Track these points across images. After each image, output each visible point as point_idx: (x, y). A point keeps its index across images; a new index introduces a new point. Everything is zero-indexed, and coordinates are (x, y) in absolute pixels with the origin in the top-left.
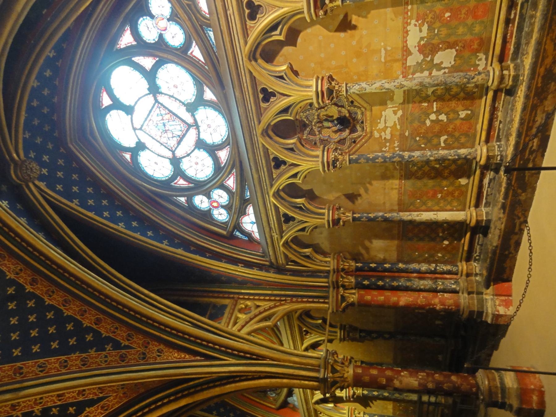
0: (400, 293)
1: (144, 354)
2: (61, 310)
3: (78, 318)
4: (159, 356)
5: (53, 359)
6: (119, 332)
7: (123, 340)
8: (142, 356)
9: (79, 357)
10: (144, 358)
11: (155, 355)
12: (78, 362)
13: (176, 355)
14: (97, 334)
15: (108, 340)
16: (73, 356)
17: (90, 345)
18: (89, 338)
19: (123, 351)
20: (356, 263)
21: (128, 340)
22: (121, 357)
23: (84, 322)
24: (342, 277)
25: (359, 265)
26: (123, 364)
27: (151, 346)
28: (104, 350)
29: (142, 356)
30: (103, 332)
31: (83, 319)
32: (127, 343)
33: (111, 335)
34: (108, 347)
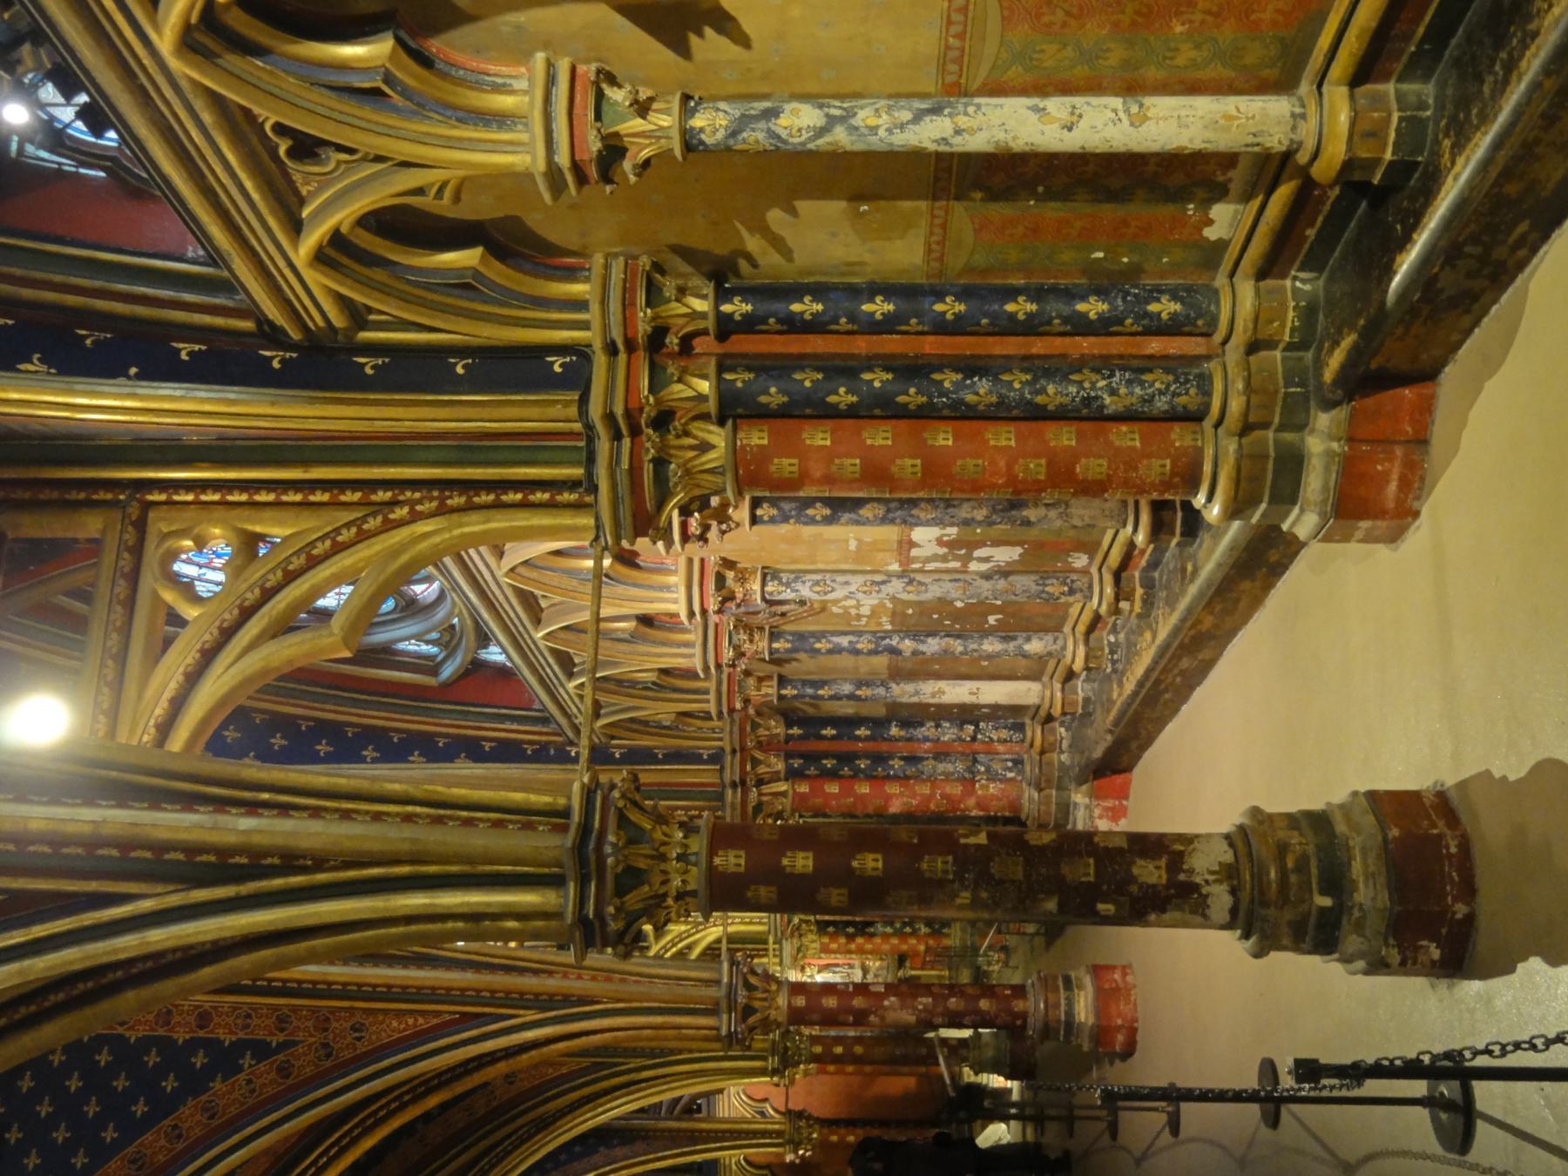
0: (893, 789)
1: (325, 1045)
2: (121, 1036)
3: (161, 1032)
4: (359, 1039)
5: (148, 1137)
6: (256, 1021)
7: (271, 1034)
8: (322, 1052)
9: (195, 1106)
10: (329, 1056)
11: (349, 1039)
12: (198, 1117)
13: (395, 1024)
14: (211, 1045)
15: (240, 1047)
16: (185, 1111)
17: (209, 1073)
18: (199, 1060)
19: (281, 1057)
20: (789, 725)
21: (282, 1030)
22: (280, 1070)
23: (175, 1036)
24: (756, 763)
25: (796, 731)
26: (290, 1082)
27: (335, 1024)
28: (240, 1069)
29: (322, 1052)
30: (222, 1037)
31: (171, 1030)
32: (281, 1038)
33: (241, 1035)
34: (247, 1061)
